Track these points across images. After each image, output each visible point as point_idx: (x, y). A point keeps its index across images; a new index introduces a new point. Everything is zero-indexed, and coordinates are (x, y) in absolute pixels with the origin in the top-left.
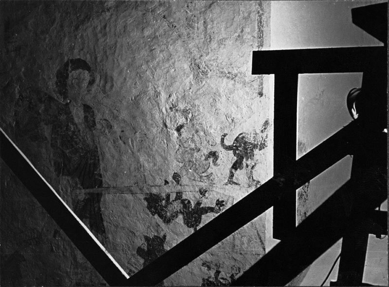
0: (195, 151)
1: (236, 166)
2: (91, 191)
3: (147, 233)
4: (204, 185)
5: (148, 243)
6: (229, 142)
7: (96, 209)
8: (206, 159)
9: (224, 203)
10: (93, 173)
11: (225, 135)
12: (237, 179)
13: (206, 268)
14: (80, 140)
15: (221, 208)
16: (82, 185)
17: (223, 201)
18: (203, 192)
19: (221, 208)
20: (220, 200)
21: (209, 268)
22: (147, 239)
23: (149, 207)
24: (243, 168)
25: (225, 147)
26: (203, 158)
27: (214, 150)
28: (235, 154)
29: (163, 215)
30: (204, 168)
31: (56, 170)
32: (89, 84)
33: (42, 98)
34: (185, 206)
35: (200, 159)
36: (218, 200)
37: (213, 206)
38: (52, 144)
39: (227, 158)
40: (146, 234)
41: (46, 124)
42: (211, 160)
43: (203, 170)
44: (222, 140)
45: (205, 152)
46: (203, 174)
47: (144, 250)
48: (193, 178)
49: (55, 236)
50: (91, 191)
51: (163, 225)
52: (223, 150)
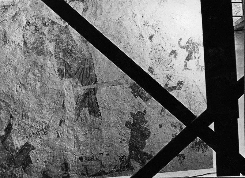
0: (162, 51)
1: (188, 59)
2: (89, 87)
3: (133, 111)
4: (169, 73)
5: (133, 117)
6: (183, 43)
7: (93, 100)
8: (170, 56)
9: (183, 83)
10: (90, 75)
12: (189, 66)
13: (174, 127)
14: (78, 52)
15: (181, 86)
16: (82, 84)
17: (182, 82)
18: (169, 77)
19: (181, 86)
20: (180, 81)
21: (176, 127)
22: (132, 115)
23: (133, 93)
24: (192, 59)
25: (181, 47)
26: (168, 55)
27: (174, 49)
29: (143, 96)
30: (169, 62)
31: (59, 75)
32: (83, 11)
33: (46, 23)
35: (166, 56)
36: (179, 81)
38: (55, 56)
40: (132, 112)
41: (50, 42)
42: (172, 56)
43: (168, 63)
44: (179, 42)
45: (169, 51)
46: (168, 66)
47: (131, 123)
48: (162, 69)
49: (60, 125)
50: (89, 87)
51: (143, 103)
52: (180, 49)
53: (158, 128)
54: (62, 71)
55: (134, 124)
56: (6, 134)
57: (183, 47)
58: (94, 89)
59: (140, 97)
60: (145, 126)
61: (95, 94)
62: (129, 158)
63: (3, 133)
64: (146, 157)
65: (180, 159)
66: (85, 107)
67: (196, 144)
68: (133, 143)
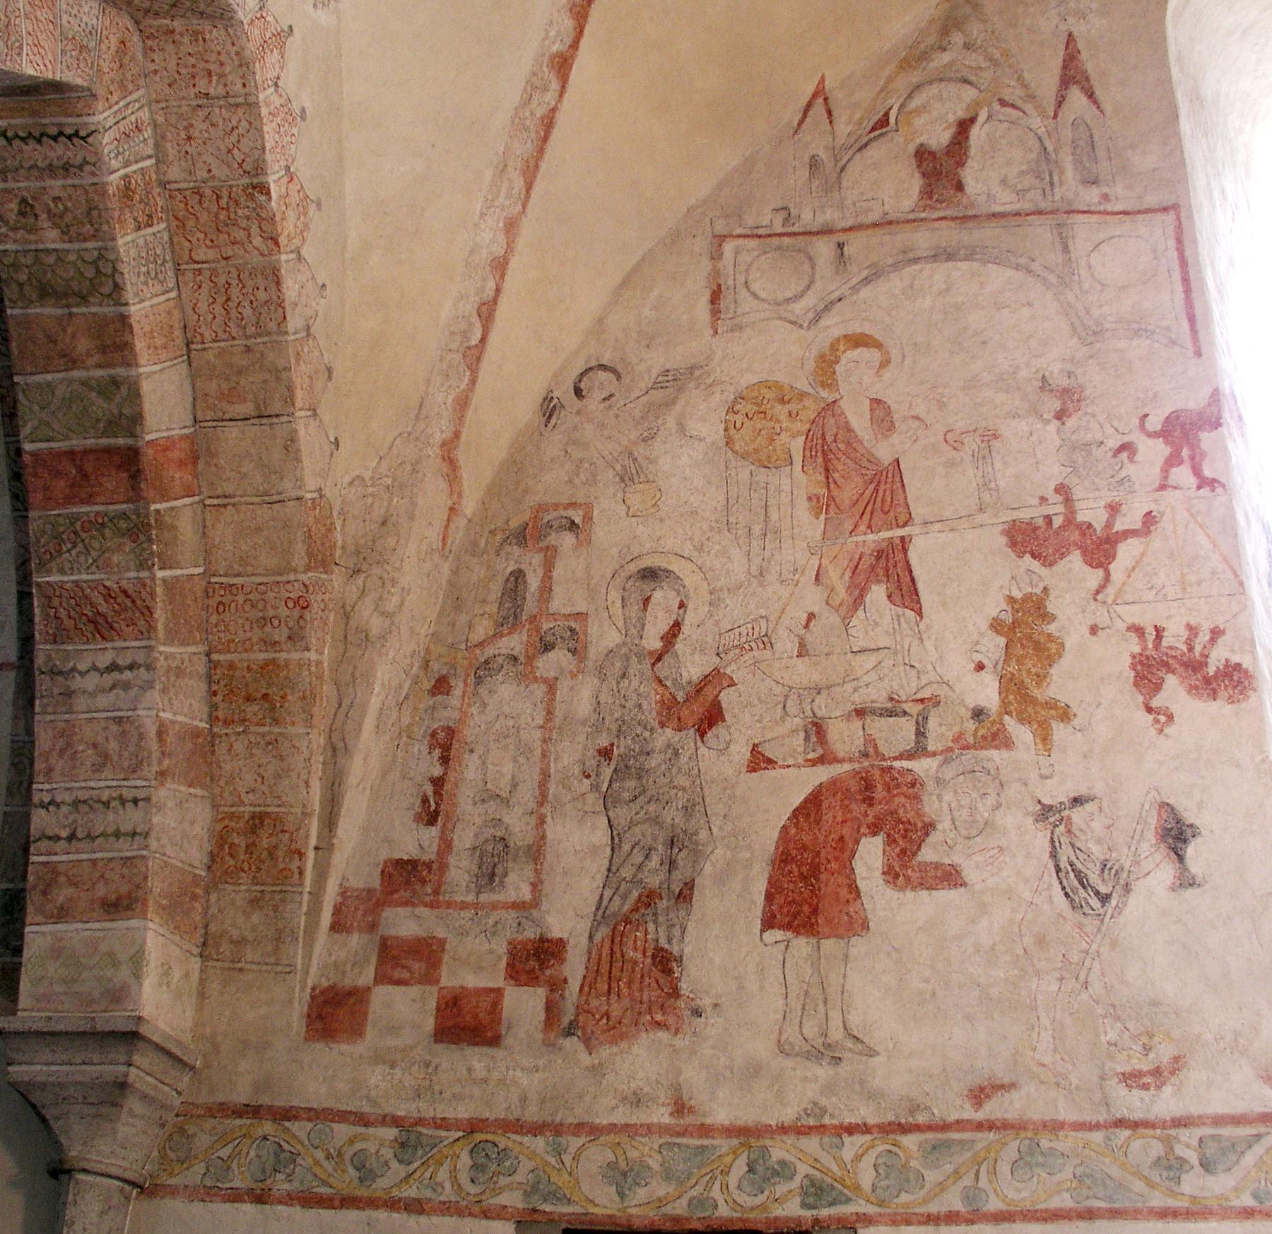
1: (1172, 461)
6: (1155, 423)
8: (1115, 456)
11: (1146, 416)
18: (1114, 509)
22: (1011, 600)
23: (1013, 544)
26: (1110, 454)
28: (1166, 443)
34: (1083, 534)
37: (1138, 526)
39: (1153, 452)
42: (1124, 455)
45: (1114, 443)
51: (1044, 571)
52: (1143, 438)
53: (1088, 635)
54: (818, 499)
55: (1015, 624)
56: (665, 646)
57: (1151, 435)
58: (902, 538)
59: (1034, 556)
60: (1052, 628)
61: (905, 550)
62: (1000, 715)
63: (658, 645)
64: (1053, 712)
65: (1157, 721)
66: (879, 582)
67: (1207, 681)
68: (1013, 674)
